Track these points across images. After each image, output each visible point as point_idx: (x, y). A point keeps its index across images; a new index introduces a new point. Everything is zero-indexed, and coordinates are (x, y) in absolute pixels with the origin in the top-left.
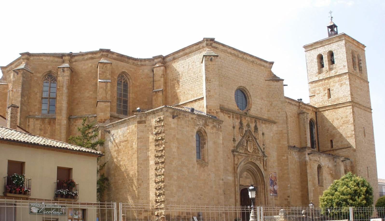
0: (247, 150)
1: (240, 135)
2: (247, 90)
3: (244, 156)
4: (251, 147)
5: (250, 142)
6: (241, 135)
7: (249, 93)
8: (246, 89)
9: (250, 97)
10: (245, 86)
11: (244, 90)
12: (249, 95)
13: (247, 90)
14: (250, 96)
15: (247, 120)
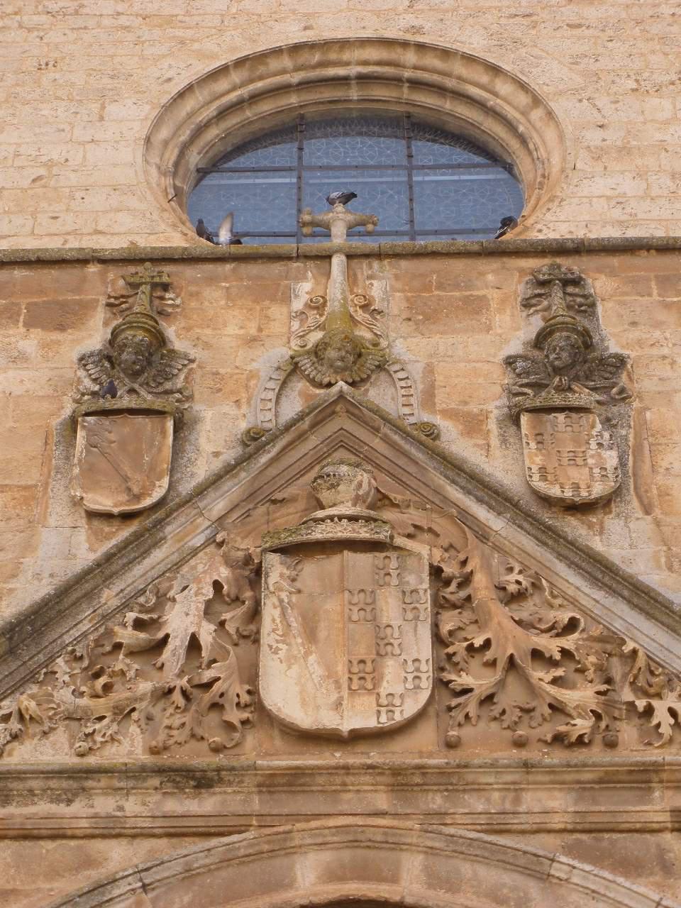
0: (256, 704)
1: (58, 513)
2: (459, 68)
3: (111, 830)
4: (382, 645)
5: (311, 569)
6: (92, 515)
7: (504, 88)
8: (446, 53)
9: (537, 114)
10: (418, 30)
11: (416, 84)
12: (523, 99)
13: (459, 68)
14: (537, 101)
15: (317, 305)
